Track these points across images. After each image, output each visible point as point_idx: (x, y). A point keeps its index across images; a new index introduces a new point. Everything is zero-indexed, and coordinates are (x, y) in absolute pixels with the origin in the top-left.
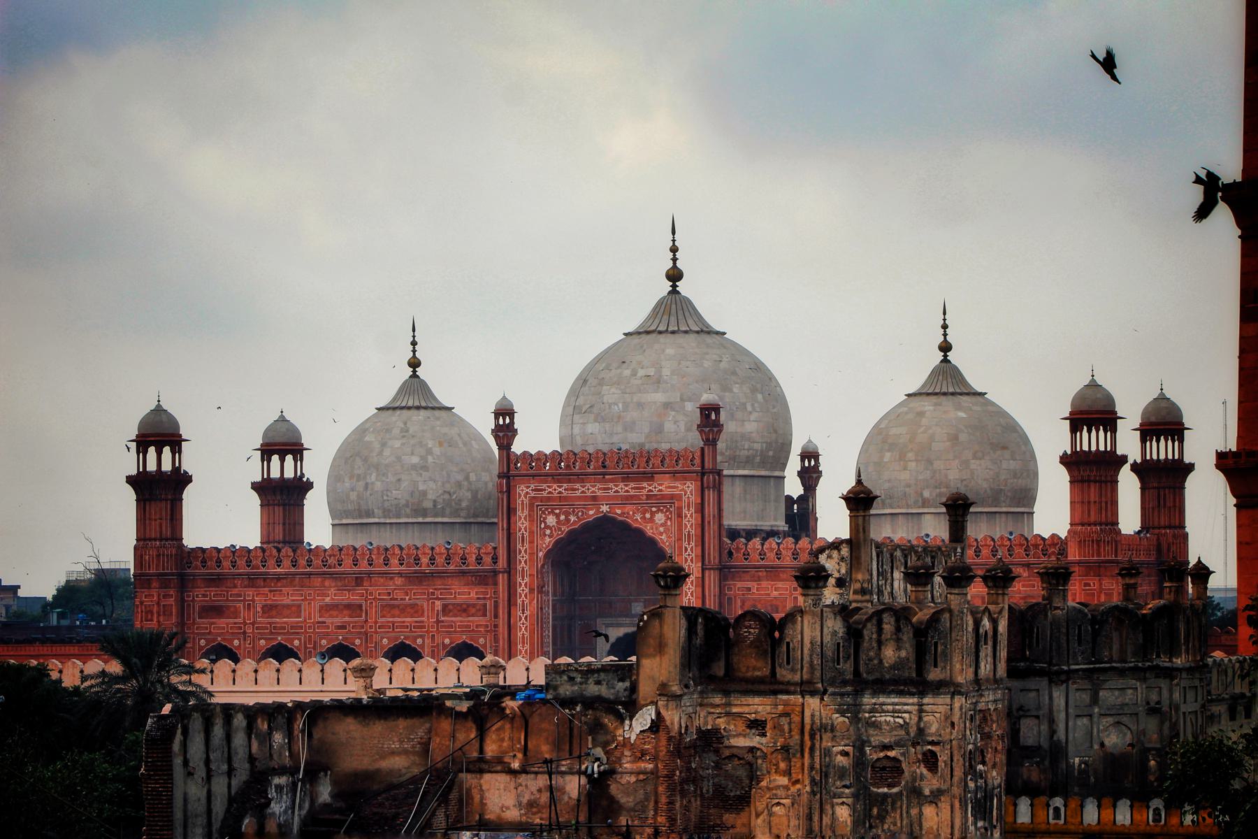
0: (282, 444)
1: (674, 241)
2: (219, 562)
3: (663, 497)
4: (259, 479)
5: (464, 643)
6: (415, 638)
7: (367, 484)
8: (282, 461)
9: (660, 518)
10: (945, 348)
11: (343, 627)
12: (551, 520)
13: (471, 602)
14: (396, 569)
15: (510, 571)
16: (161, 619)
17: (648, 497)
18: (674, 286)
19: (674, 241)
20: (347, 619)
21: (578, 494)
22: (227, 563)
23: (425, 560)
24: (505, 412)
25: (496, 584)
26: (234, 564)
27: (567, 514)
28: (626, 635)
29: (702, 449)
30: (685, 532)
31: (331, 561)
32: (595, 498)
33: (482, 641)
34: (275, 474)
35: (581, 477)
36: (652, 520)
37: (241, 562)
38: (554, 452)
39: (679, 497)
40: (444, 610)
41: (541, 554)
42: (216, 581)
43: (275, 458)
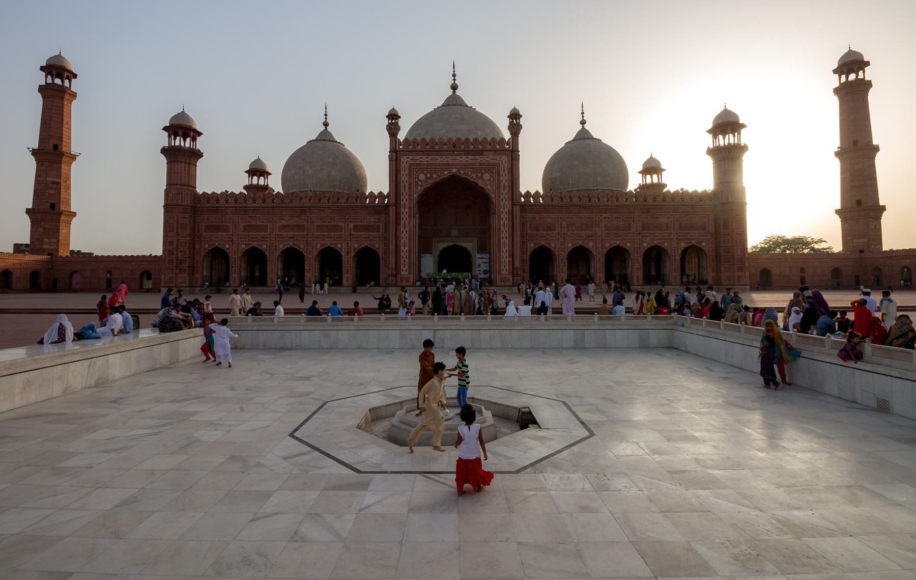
0: (257, 170)
2: (218, 201)
3: (489, 164)
6: (337, 244)
9: (487, 176)
10: (583, 122)
12: (422, 177)
14: (325, 205)
15: (397, 204)
16: (179, 231)
17: (480, 164)
18: (454, 92)
21: (438, 162)
22: (222, 201)
23: (344, 200)
24: (393, 116)
25: (387, 214)
26: (227, 201)
27: (431, 173)
28: (449, 247)
30: (502, 184)
32: (448, 165)
33: (377, 246)
35: (440, 152)
36: (482, 178)
37: (231, 201)
38: (424, 140)
39: (498, 165)
43: (255, 178)
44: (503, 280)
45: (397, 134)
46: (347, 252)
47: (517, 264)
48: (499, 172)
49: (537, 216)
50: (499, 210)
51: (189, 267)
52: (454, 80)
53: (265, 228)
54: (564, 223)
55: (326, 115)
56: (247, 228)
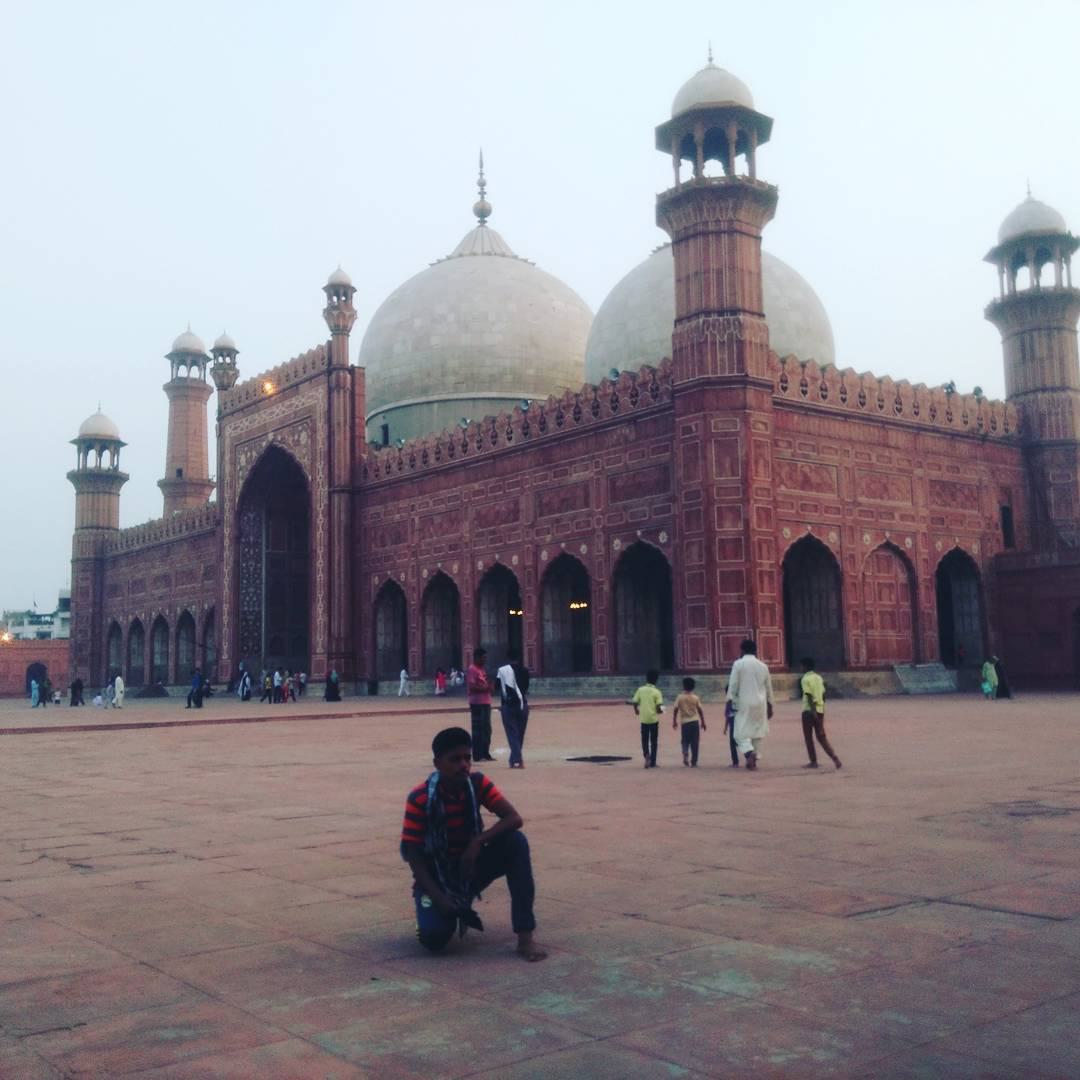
1: (481, 174)
11: (161, 598)
12: (243, 459)
17: (295, 413)
18: (483, 222)
19: (481, 174)
21: (256, 425)
23: (197, 523)
29: (329, 342)
36: (297, 443)
40: (205, 574)
48: (314, 422)
49: (379, 508)
51: (92, 654)
52: (482, 193)
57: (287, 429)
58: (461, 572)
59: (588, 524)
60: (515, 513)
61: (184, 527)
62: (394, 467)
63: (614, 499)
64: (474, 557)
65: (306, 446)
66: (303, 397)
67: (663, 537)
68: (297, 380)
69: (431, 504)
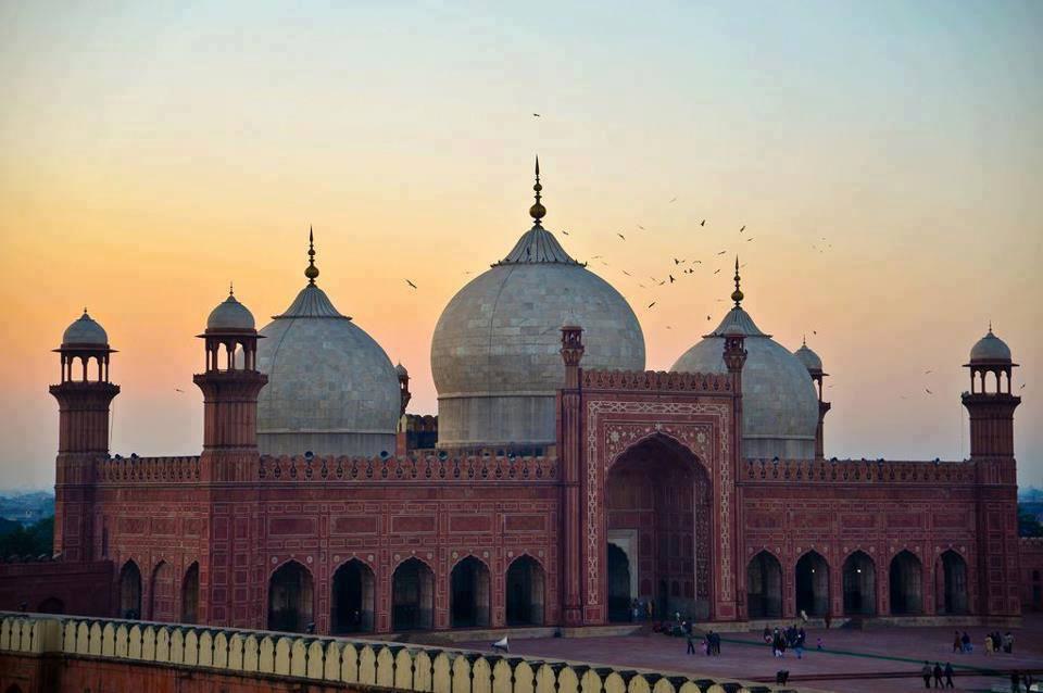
1: (538, 180)
2: (294, 472)
4: (59, 382)
5: (525, 555)
7: (342, 395)
8: (85, 363)
12: (615, 436)
13: (534, 514)
15: (581, 485)
17: (694, 418)
18: (538, 222)
19: (538, 180)
20: (419, 533)
21: (637, 412)
22: (301, 473)
23: (492, 473)
27: (628, 431)
30: (721, 451)
31: (406, 472)
32: (651, 417)
33: (541, 554)
34: (77, 377)
36: (695, 439)
39: (716, 419)
41: (606, 469)
42: (291, 491)
43: (77, 361)
44: (726, 611)
45: (576, 363)
46: (497, 563)
47: (742, 584)
48: (717, 429)
50: (718, 495)
52: (538, 197)
53: (370, 524)
54: (792, 514)
55: (312, 253)
56: (342, 525)
57: (681, 426)
58: (831, 552)
59: (921, 536)
60: (872, 522)
61: (465, 473)
62: (770, 475)
63: (935, 526)
64: (841, 546)
65: (704, 444)
66: (703, 406)
67: (963, 549)
68: (694, 392)
69: (805, 505)
